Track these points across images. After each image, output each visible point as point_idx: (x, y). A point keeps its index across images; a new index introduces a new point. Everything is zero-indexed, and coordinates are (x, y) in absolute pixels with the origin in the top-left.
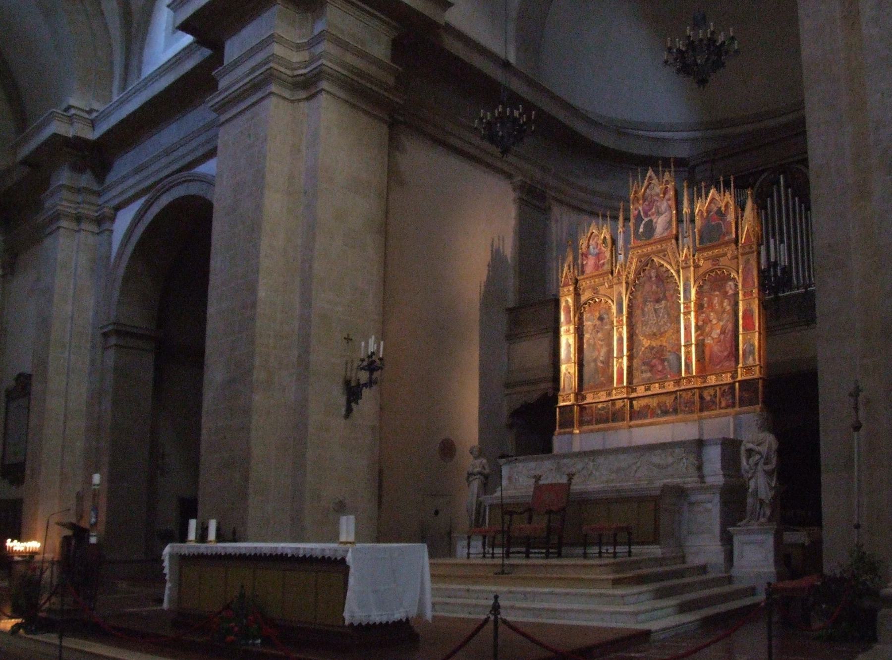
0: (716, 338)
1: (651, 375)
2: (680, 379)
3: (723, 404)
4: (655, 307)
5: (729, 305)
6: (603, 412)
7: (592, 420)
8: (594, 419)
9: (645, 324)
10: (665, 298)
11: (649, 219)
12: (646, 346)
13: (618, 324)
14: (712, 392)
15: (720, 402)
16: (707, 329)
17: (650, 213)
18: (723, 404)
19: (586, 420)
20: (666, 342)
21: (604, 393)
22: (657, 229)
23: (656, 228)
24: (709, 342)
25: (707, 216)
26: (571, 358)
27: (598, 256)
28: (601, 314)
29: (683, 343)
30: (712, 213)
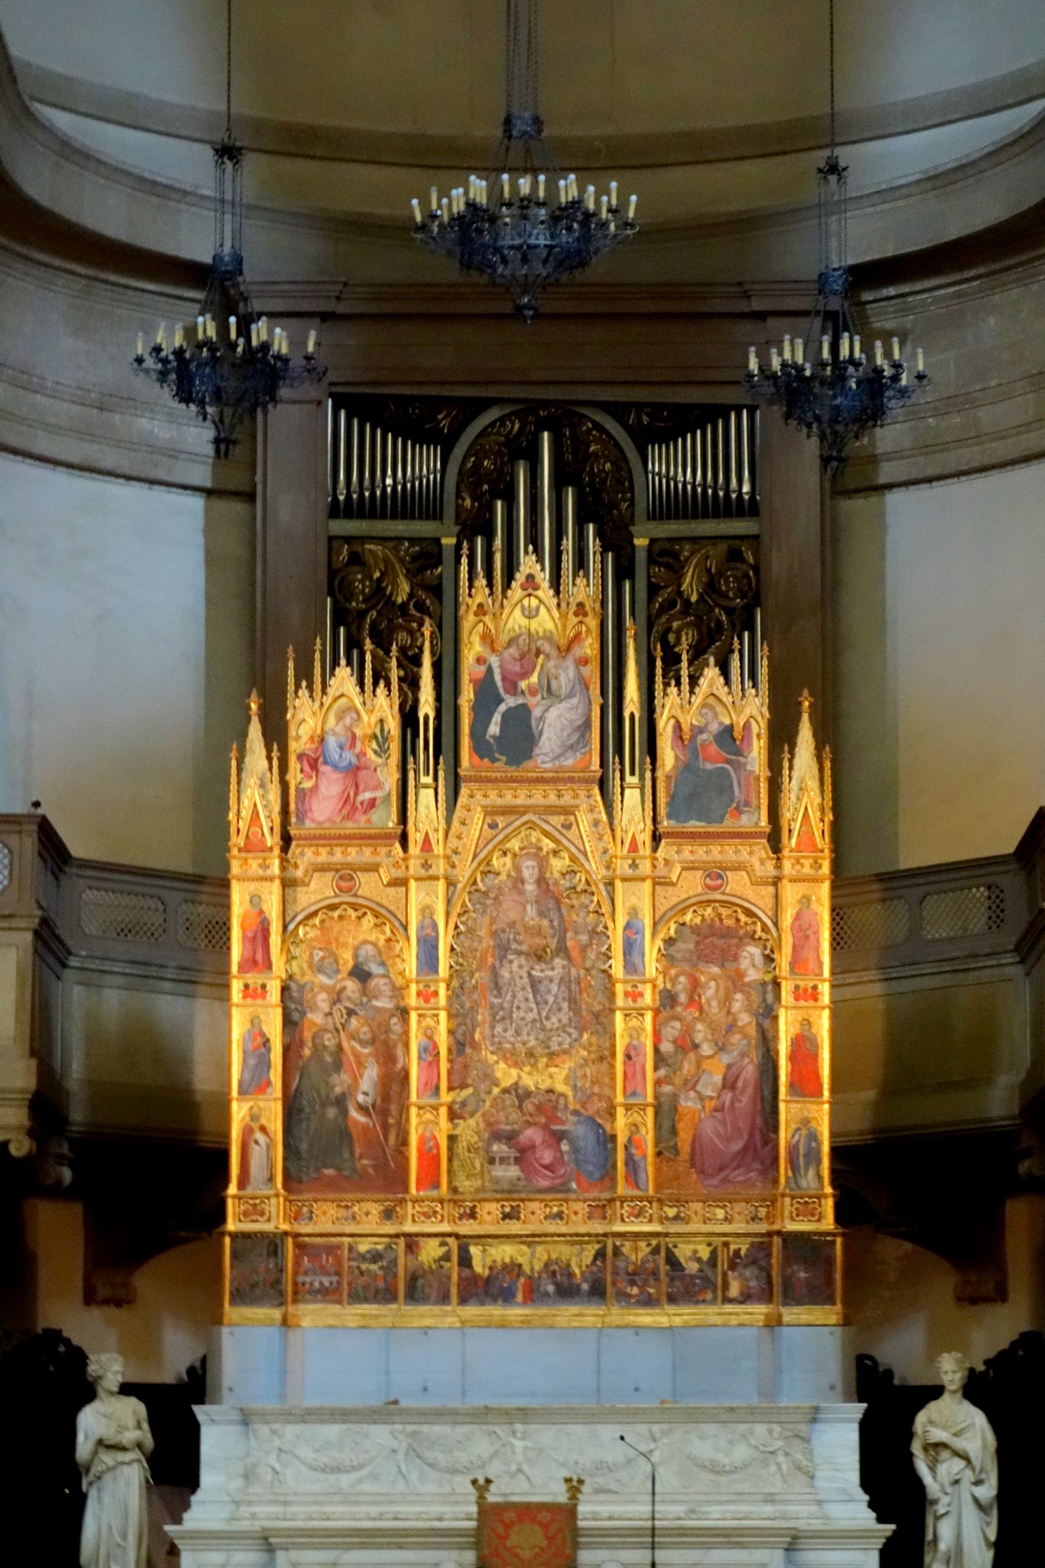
0: (711, 1098)
1: (519, 1173)
2: (612, 1200)
3: (734, 1290)
4: (534, 973)
5: (747, 1011)
6: (374, 1267)
8: (345, 1286)
9: (500, 1016)
10: (562, 950)
11: (520, 701)
12: (506, 1083)
13: (423, 1004)
14: (705, 1253)
15: (726, 1286)
16: (688, 1067)
17: (523, 685)
18: (734, 1290)
19: (317, 1285)
21: (375, 1209)
22: (544, 738)
23: (541, 733)
24: (690, 1104)
25: (693, 738)
26: (269, 1083)
27: (354, 772)
28: (360, 959)
29: (619, 1098)
30: (704, 736)
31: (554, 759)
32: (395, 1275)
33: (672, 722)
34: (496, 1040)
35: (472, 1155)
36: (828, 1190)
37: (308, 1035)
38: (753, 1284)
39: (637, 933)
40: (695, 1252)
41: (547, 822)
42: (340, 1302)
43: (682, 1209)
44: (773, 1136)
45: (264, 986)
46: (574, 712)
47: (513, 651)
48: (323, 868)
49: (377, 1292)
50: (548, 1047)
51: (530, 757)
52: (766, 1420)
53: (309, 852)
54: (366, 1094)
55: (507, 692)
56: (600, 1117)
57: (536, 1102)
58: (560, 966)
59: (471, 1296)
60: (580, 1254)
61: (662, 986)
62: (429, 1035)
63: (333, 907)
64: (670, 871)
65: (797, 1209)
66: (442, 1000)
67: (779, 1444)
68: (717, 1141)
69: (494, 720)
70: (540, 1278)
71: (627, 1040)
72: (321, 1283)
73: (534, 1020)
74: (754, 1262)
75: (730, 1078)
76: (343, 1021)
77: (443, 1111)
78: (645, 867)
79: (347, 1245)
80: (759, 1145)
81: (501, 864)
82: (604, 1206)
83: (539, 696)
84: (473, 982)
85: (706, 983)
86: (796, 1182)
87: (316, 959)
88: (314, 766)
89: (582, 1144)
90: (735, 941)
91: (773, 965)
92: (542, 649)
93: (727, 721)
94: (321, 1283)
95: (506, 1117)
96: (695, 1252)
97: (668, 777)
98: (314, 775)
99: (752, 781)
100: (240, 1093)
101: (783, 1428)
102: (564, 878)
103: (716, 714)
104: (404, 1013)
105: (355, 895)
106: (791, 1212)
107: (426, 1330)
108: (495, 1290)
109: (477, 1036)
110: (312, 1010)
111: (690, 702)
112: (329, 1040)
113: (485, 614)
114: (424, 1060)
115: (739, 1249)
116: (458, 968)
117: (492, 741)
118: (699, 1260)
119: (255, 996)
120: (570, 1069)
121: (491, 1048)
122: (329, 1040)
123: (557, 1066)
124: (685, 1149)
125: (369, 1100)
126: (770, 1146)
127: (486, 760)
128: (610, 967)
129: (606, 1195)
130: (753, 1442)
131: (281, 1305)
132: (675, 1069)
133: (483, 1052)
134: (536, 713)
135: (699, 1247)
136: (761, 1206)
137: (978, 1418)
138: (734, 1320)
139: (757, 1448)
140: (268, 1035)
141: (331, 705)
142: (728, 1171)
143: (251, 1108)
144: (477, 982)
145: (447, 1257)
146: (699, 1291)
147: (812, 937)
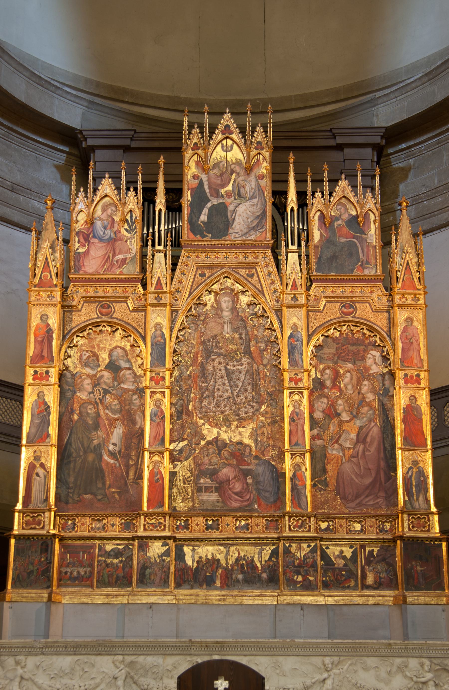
0: (349, 448)
3: (370, 579)
4: (229, 367)
6: (115, 561)
7: (92, 573)
10: (247, 352)
11: (221, 201)
13: (154, 385)
14: (348, 552)
15: (364, 577)
16: (333, 428)
17: (223, 191)
18: (370, 579)
19: (75, 574)
20: (251, 436)
21: (117, 521)
22: (235, 223)
24: (334, 452)
26: (48, 435)
28: (113, 358)
29: (287, 446)
30: (339, 222)
31: (242, 236)
32: (131, 567)
33: (318, 213)
34: (203, 410)
35: (186, 486)
36: (434, 509)
37: (76, 406)
38: (382, 575)
39: (297, 341)
40: (342, 552)
41: (238, 273)
42: (92, 587)
43: (331, 523)
44: (393, 474)
45: (47, 372)
46: (255, 207)
47: (216, 171)
48: (89, 300)
49: (118, 579)
50: (238, 415)
51: (227, 235)
52: (418, 655)
53: (81, 290)
54: (114, 444)
55: (212, 195)
56: (274, 460)
57: (230, 450)
58: (246, 363)
59: (185, 582)
60: (260, 553)
61: (314, 376)
62: (158, 404)
63: (97, 325)
64: (319, 303)
65: (412, 522)
66: (167, 383)
67: (429, 676)
68: (353, 477)
69: (203, 213)
70: (232, 569)
71: (291, 409)
72: (78, 572)
73: (229, 398)
74: (384, 560)
75: (362, 436)
76: (101, 397)
77: (167, 454)
78: (302, 299)
79: (97, 545)
80: (383, 480)
81: (209, 299)
82: (277, 520)
83: (233, 198)
84: (188, 373)
85: (344, 374)
86: (411, 504)
87: (84, 357)
88: (87, 239)
89: (261, 479)
90: (362, 347)
91: (389, 362)
92: (235, 170)
93: (354, 213)
94: (78, 572)
95: (210, 460)
96: (342, 552)
97: (316, 247)
98: (87, 244)
99: (371, 248)
100: (27, 442)
101: (431, 662)
102: (249, 308)
103: (346, 209)
104: (141, 392)
105: (111, 317)
106: (409, 525)
107: (151, 606)
108: (201, 578)
109: (190, 407)
110: (80, 390)
111: (330, 201)
112: (91, 409)
113: (198, 149)
114: (155, 421)
115: (373, 550)
116: (178, 363)
117: (202, 224)
118: (344, 558)
119: (41, 379)
120: (253, 429)
121: (200, 415)
122: (91, 410)
123: (244, 427)
124: (332, 482)
125: (117, 449)
126: (391, 481)
127: (198, 236)
128: (280, 363)
129: (279, 513)
130: (408, 674)
131: (48, 587)
132: (325, 428)
133: (195, 418)
134: (231, 208)
135: (344, 549)
136: (386, 522)
138: (371, 601)
139: (411, 679)
140: (49, 404)
141: (99, 202)
142: (362, 497)
143: (35, 451)
144: (190, 371)
145: (167, 553)
146: (345, 580)
147: (415, 343)
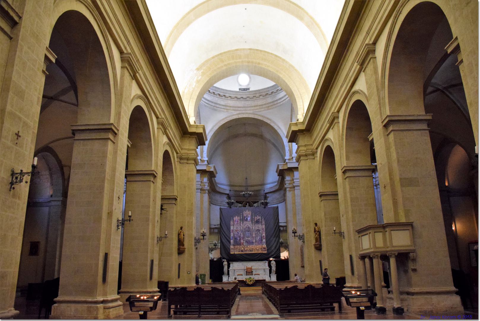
137: (274, 262)
